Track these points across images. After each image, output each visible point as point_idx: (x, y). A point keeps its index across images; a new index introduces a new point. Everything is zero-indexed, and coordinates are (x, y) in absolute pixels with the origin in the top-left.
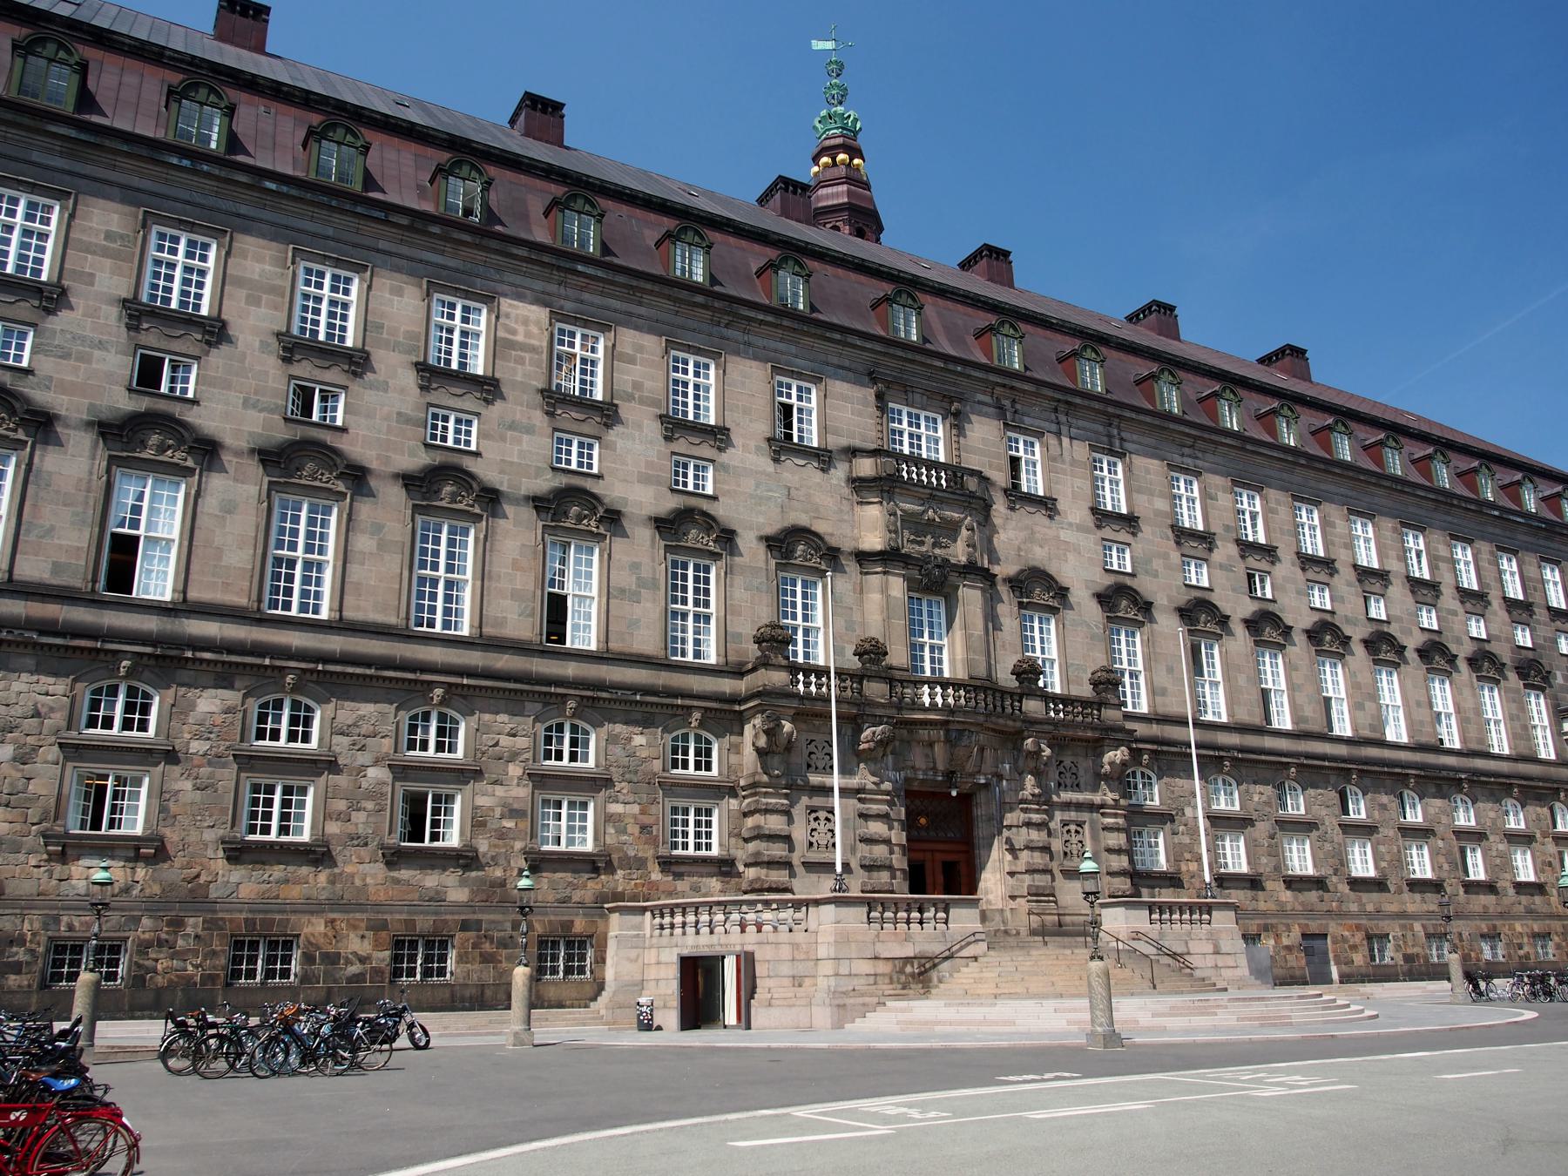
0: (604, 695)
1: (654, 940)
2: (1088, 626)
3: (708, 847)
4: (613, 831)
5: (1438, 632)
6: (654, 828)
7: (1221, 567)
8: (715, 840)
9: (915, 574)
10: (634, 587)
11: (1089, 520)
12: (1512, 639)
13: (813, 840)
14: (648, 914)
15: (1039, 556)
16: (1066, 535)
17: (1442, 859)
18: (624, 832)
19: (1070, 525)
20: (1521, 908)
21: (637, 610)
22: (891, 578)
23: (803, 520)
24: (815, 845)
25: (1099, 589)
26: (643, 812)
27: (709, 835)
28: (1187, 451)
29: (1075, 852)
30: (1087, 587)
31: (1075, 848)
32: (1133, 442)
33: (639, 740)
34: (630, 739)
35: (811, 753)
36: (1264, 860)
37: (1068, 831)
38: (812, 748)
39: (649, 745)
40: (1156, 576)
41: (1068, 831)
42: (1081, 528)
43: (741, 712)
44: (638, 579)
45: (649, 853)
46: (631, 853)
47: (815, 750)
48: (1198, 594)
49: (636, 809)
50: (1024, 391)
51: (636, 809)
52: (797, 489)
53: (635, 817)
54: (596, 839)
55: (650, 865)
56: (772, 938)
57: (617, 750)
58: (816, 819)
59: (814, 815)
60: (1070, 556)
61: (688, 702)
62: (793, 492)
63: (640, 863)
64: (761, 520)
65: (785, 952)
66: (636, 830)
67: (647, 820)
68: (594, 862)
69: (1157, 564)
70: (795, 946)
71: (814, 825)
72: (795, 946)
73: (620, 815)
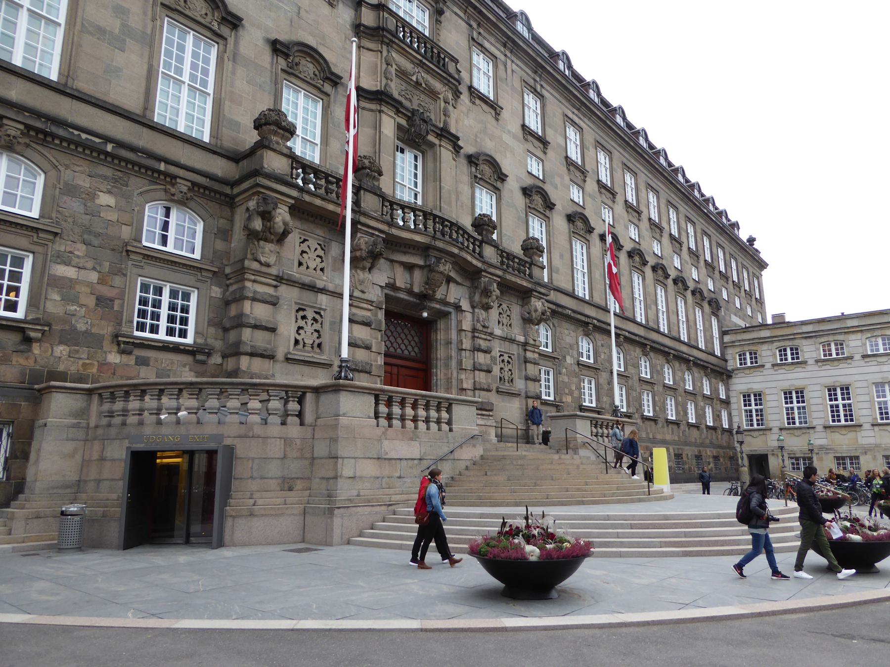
0: (61, 132)
1: (100, 431)
2: (517, 209)
3: (183, 334)
4: (57, 297)
5: (681, 271)
6: (117, 303)
7: (590, 195)
8: (191, 328)
9: (403, 122)
10: (117, 31)
11: (520, 133)
12: (707, 285)
13: (299, 338)
14: (95, 398)
15: (489, 147)
16: (506, 138)
17: (680, 408)
18: (75, 300)
19: (509, 132)
20: (708, 441)
21: (120, 59)
22: (384, 117)
23: (311, 41)
24: (301, 343)
25: (525, 185)
26: (102, 281)
27: (184, 321)
28: (576, 112)
29: (506, 378)
30: (517, 181)
31: (507, 375)
32: (547, 91)
33: (105, 199)
34: (92, 196)
35: (303, 252)
36: (605, 399)
37: (503, 361)
38: (304, 247)
39: (118, 208)
40: (556, 187)
41: (503, 361)
42: (515, 137)
43: (232, 198)
44: (124, 25)
45: (107, 330)
46: (81, 326)
47: (307, 250)
48: (579, 210)
49: (94, 277)
50: (488, 19)
51: (94, 277)
52: (307, 12)
53: (90, 284)
54: (33, 303)
55: (107, 345)
56: (258, 430)
57: (74, 205)
58: (304, 317)
59: (301, 313)
60: (509, 155)
61: (173, 170)
62: (302, 12)
63: (92, 341)
64: (270, 24)
65: (275, 449)
66: (91, 301)
67: (105, 291)
68: (22, 330)
69: (557, 180)
70: (288, 442)
71: (301, 323)
72: (288, 442)
73: (71, 280)
